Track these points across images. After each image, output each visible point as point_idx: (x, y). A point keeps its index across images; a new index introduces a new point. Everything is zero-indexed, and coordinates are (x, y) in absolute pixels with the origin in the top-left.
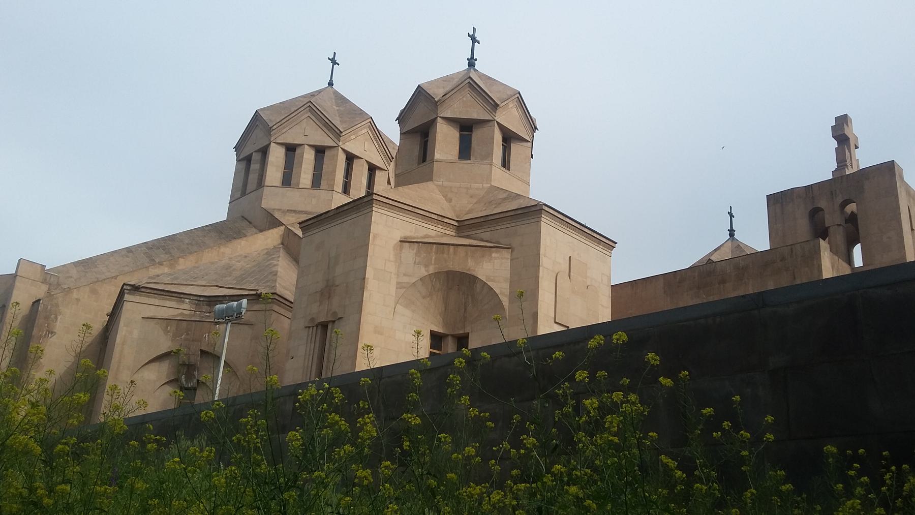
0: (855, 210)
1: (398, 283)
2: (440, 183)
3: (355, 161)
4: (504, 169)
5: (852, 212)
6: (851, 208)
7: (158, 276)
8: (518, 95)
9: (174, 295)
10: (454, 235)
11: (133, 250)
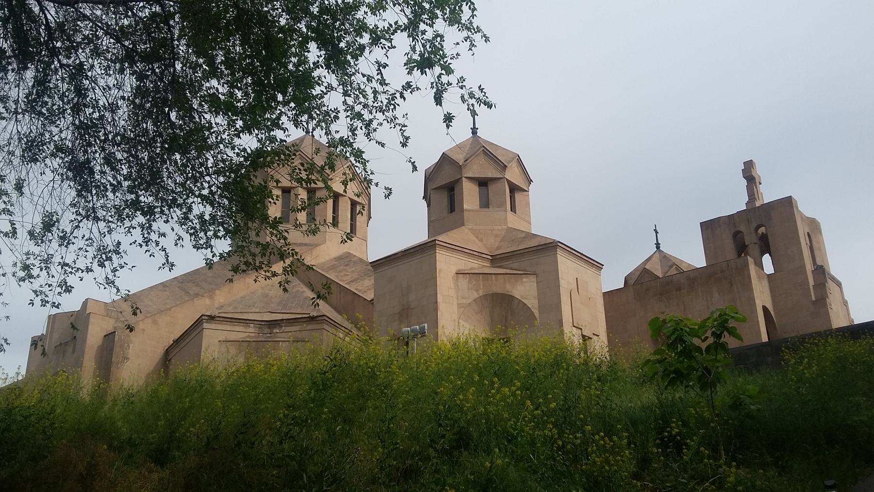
0: (764, 232)
1: (458, 304)
2: (471, 227)
3: (341, 199)
4: (511, 212)
5: (762, 233)
6: (762, 230)
7: (222, 307)
8: (518, 157)
9: (241, 321)
10: (489, 265)
11: (168, 285)
